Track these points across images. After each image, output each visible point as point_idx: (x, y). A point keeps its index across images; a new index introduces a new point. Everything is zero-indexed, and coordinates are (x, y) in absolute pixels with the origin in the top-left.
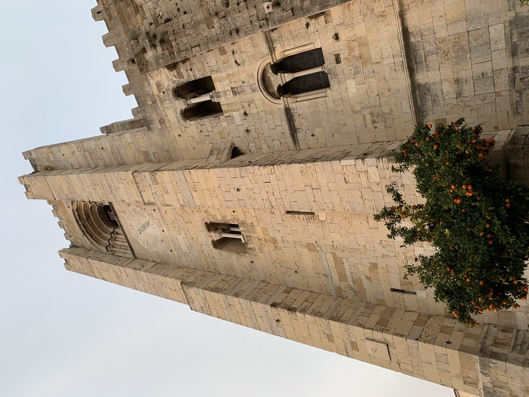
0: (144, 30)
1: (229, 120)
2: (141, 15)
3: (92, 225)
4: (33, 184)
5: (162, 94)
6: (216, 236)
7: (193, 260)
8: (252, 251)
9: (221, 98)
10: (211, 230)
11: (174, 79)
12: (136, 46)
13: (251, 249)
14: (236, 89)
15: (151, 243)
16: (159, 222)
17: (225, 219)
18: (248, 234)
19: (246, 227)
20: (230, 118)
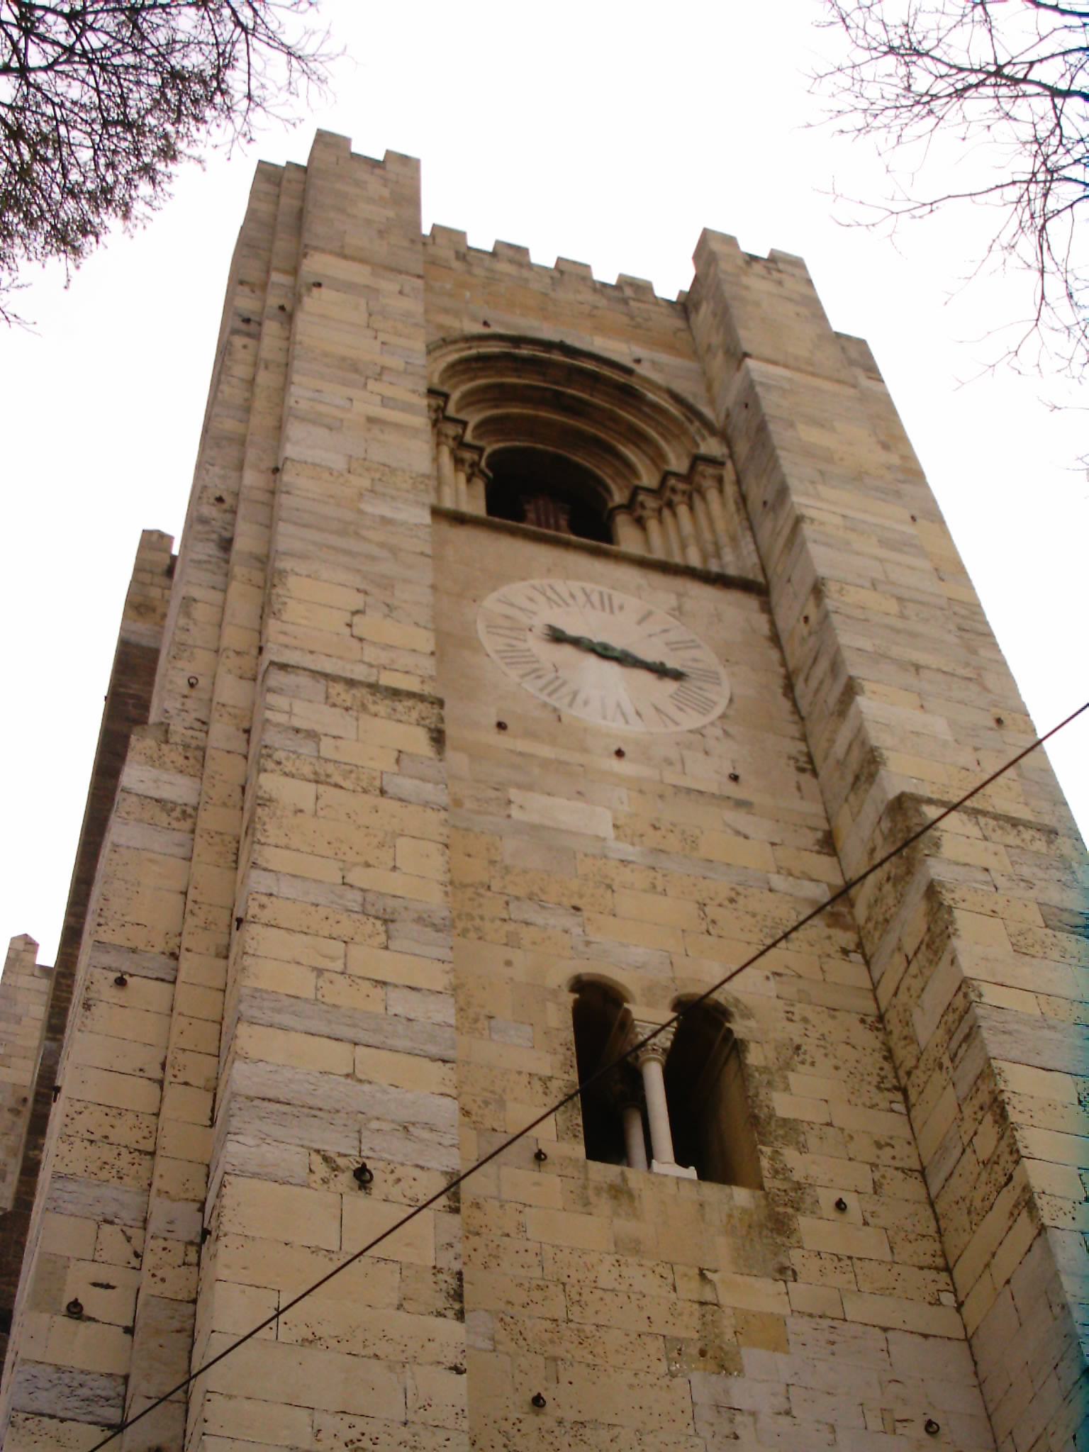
16: (670, 763)
17: (781, 1132)
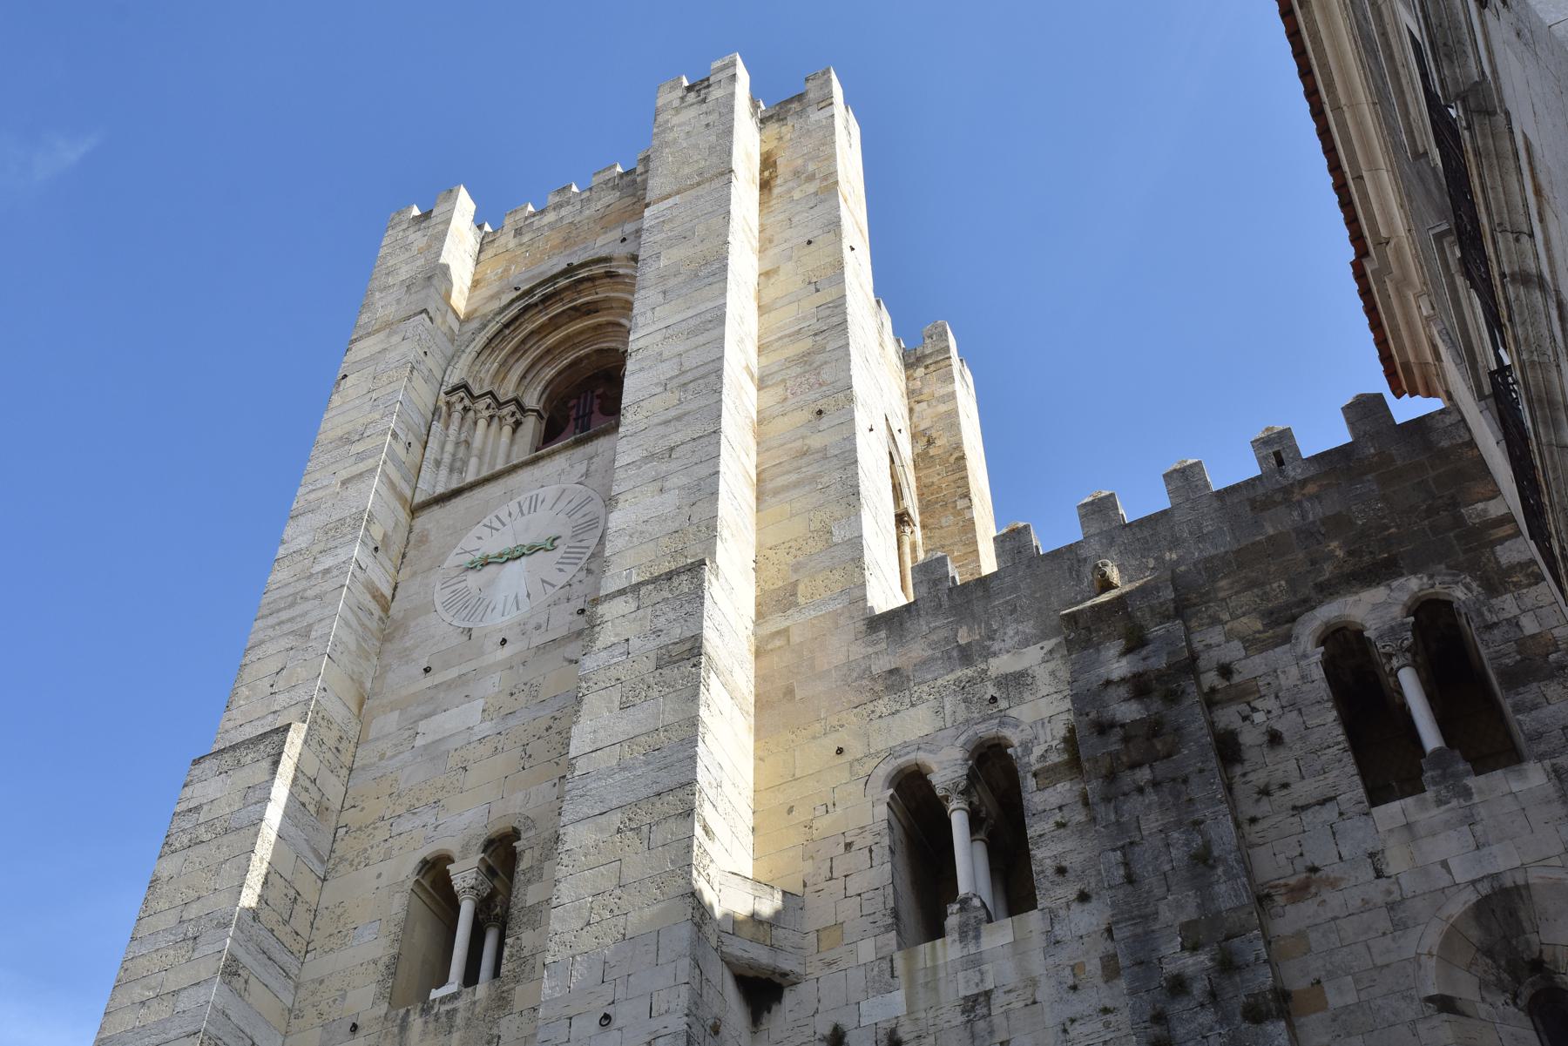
0: (1208, 641)
1: (881, 971)
2: (1259, 632)
3: (554, 324)
4: (711, 119)
5: (991, 691)
6: (464, 875)
7: (384, 763)
8: (396, 1030)
9: (958, 945)
10: (490, 851)
11: (1037, 751)
12: (1151, 608)
13: (404, 1026)
14: (985, 1011)
15: (463, 585)
17: (525, 920)
18: (459, 1020)
19: (486, 1010)
20: (887, 976)
